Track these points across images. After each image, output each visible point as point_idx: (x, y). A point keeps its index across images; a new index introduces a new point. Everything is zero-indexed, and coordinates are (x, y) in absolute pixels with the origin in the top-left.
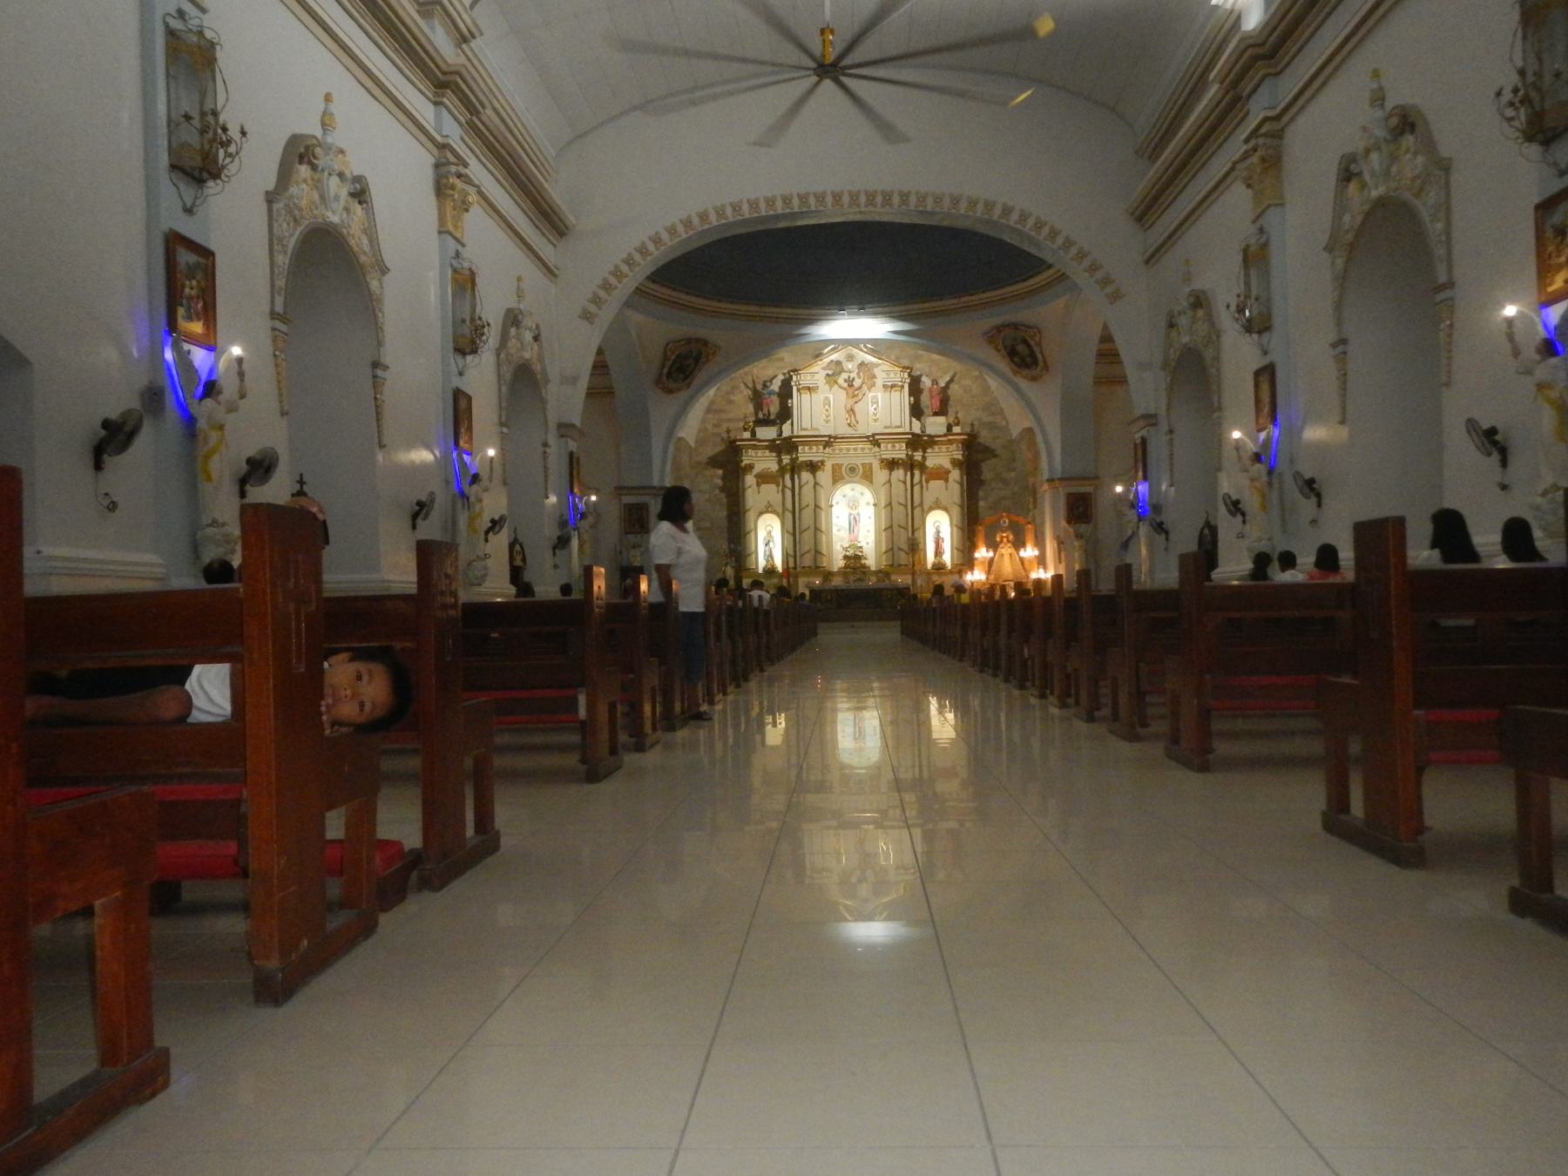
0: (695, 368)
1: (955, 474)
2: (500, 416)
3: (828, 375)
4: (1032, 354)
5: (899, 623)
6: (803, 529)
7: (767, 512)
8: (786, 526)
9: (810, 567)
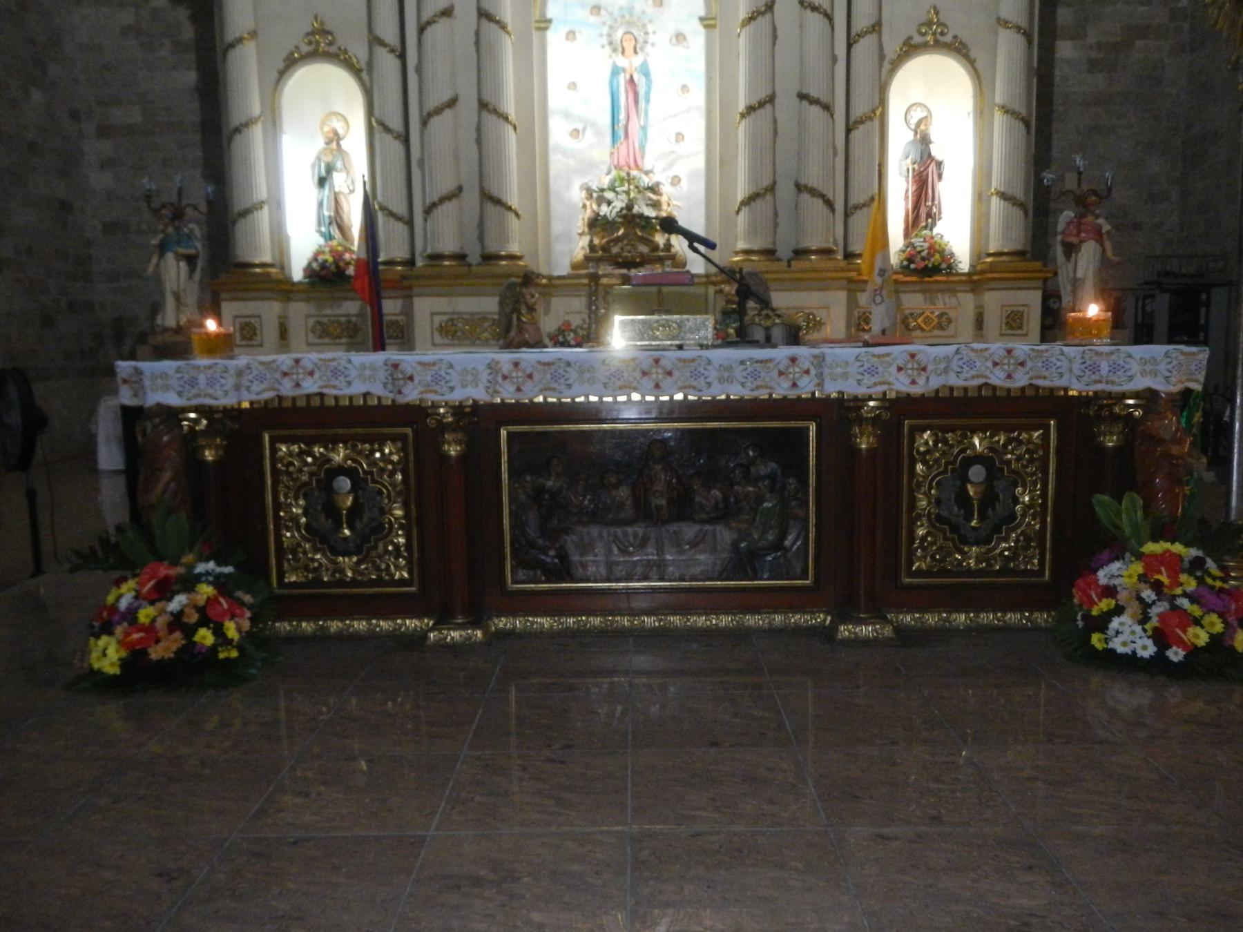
6: (433, 101)
7: (314, 55)
8: (377, 112)
9: (460, 257)
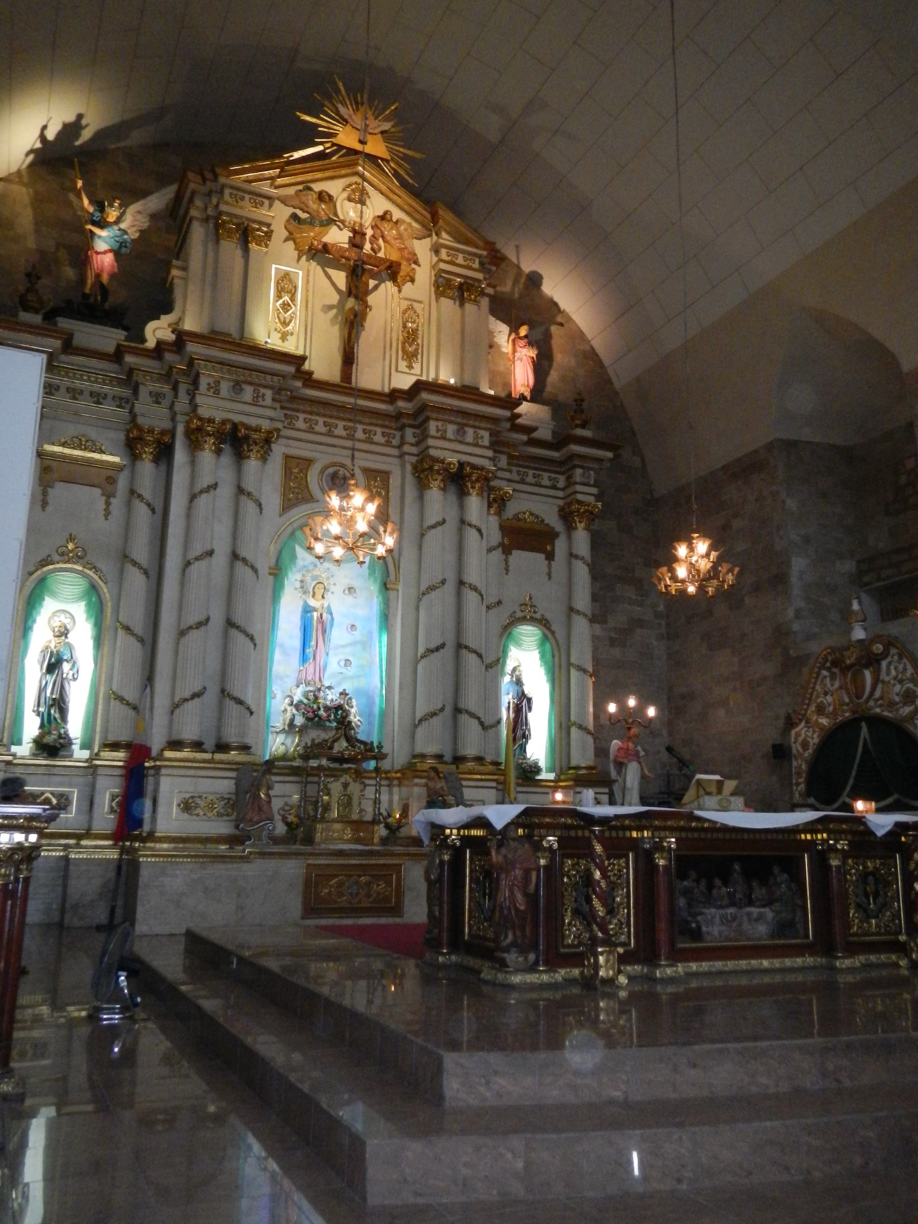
3: (295, 217)
6: (192, 618)
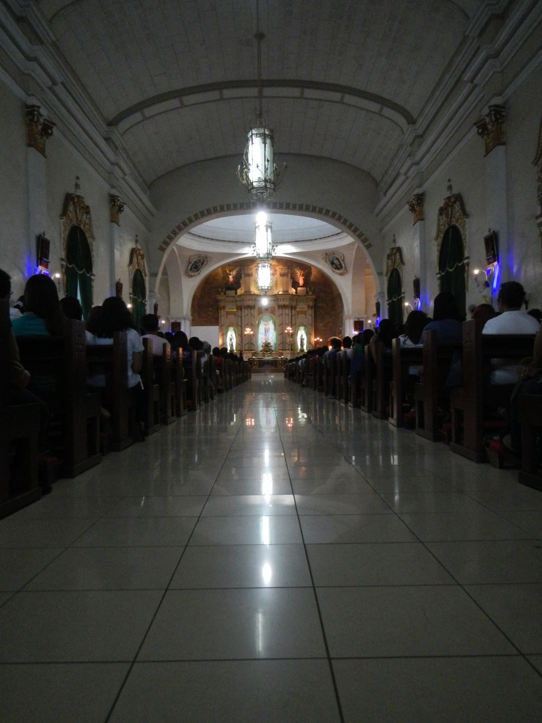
0: (201, 267)
1: (311, 312)
2: (130, 291)
4: (341, 265)
5: (283, 374)
